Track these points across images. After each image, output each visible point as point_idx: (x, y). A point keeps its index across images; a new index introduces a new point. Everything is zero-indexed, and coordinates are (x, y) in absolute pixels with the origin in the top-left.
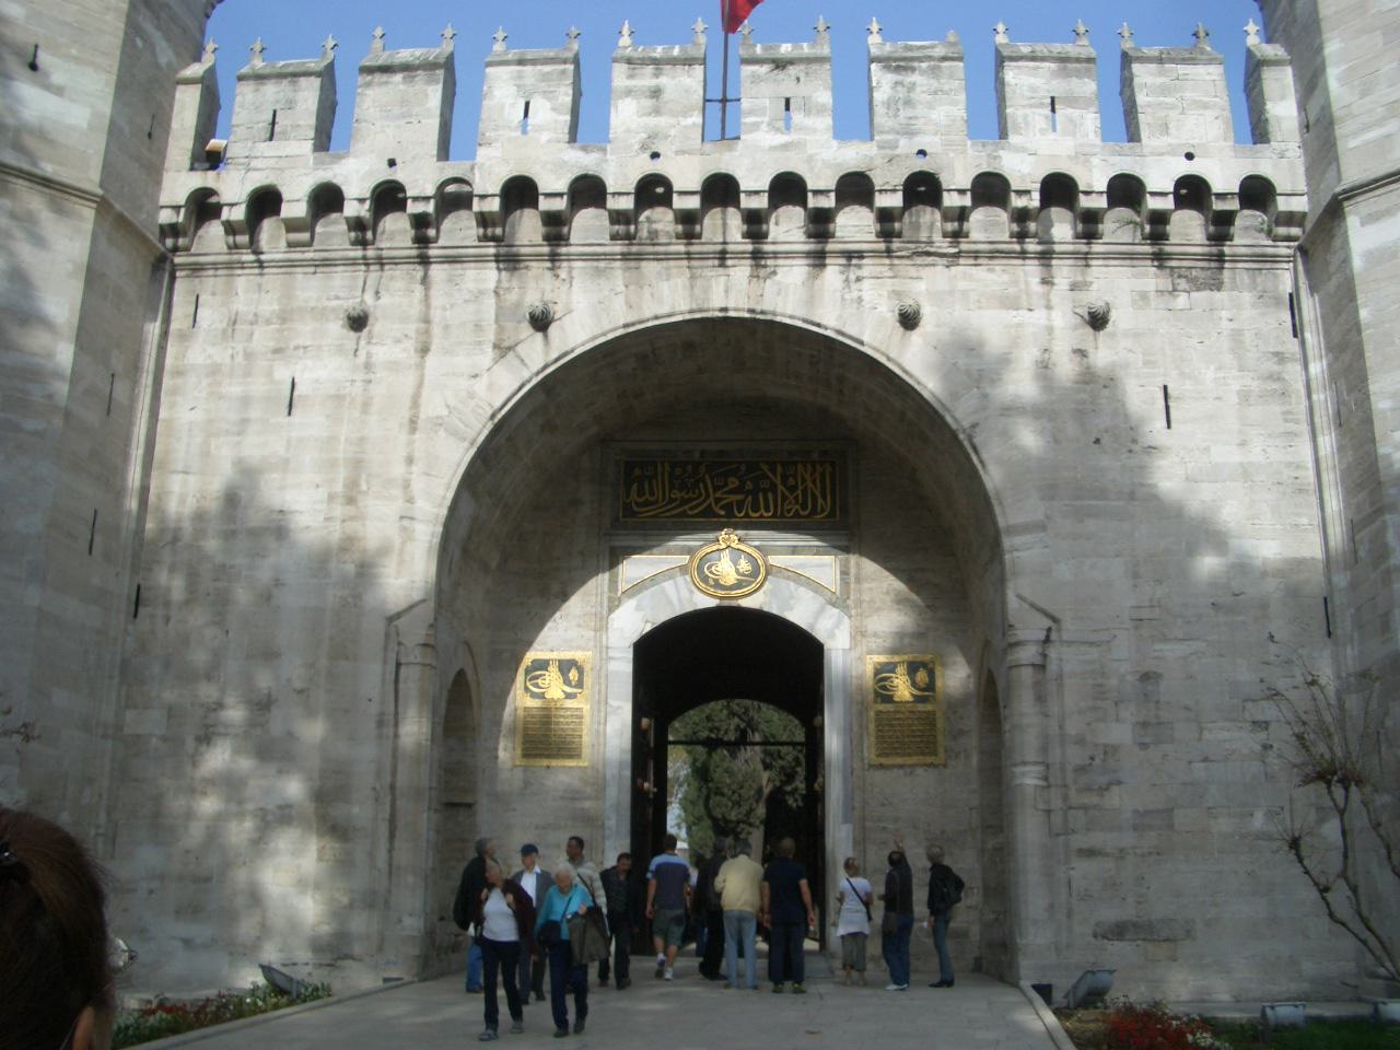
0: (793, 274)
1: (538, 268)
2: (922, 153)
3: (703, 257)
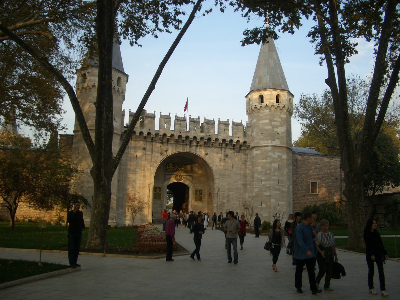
0: (194, 147)
1: (165, 144)
2: (210, 135)
3: (184, 145)
